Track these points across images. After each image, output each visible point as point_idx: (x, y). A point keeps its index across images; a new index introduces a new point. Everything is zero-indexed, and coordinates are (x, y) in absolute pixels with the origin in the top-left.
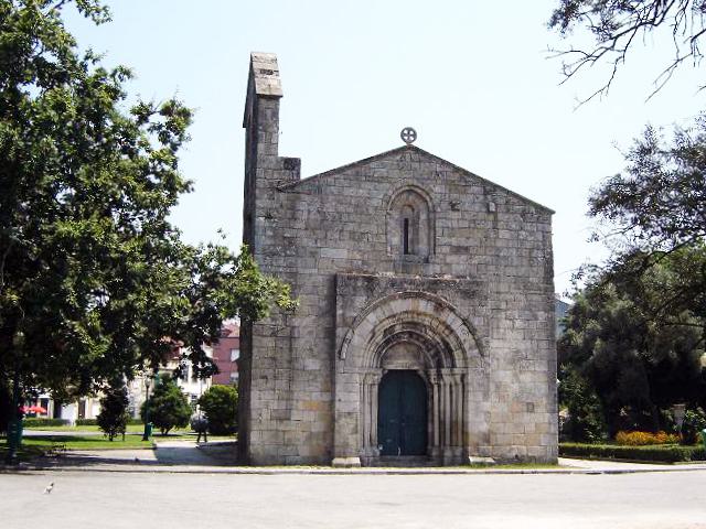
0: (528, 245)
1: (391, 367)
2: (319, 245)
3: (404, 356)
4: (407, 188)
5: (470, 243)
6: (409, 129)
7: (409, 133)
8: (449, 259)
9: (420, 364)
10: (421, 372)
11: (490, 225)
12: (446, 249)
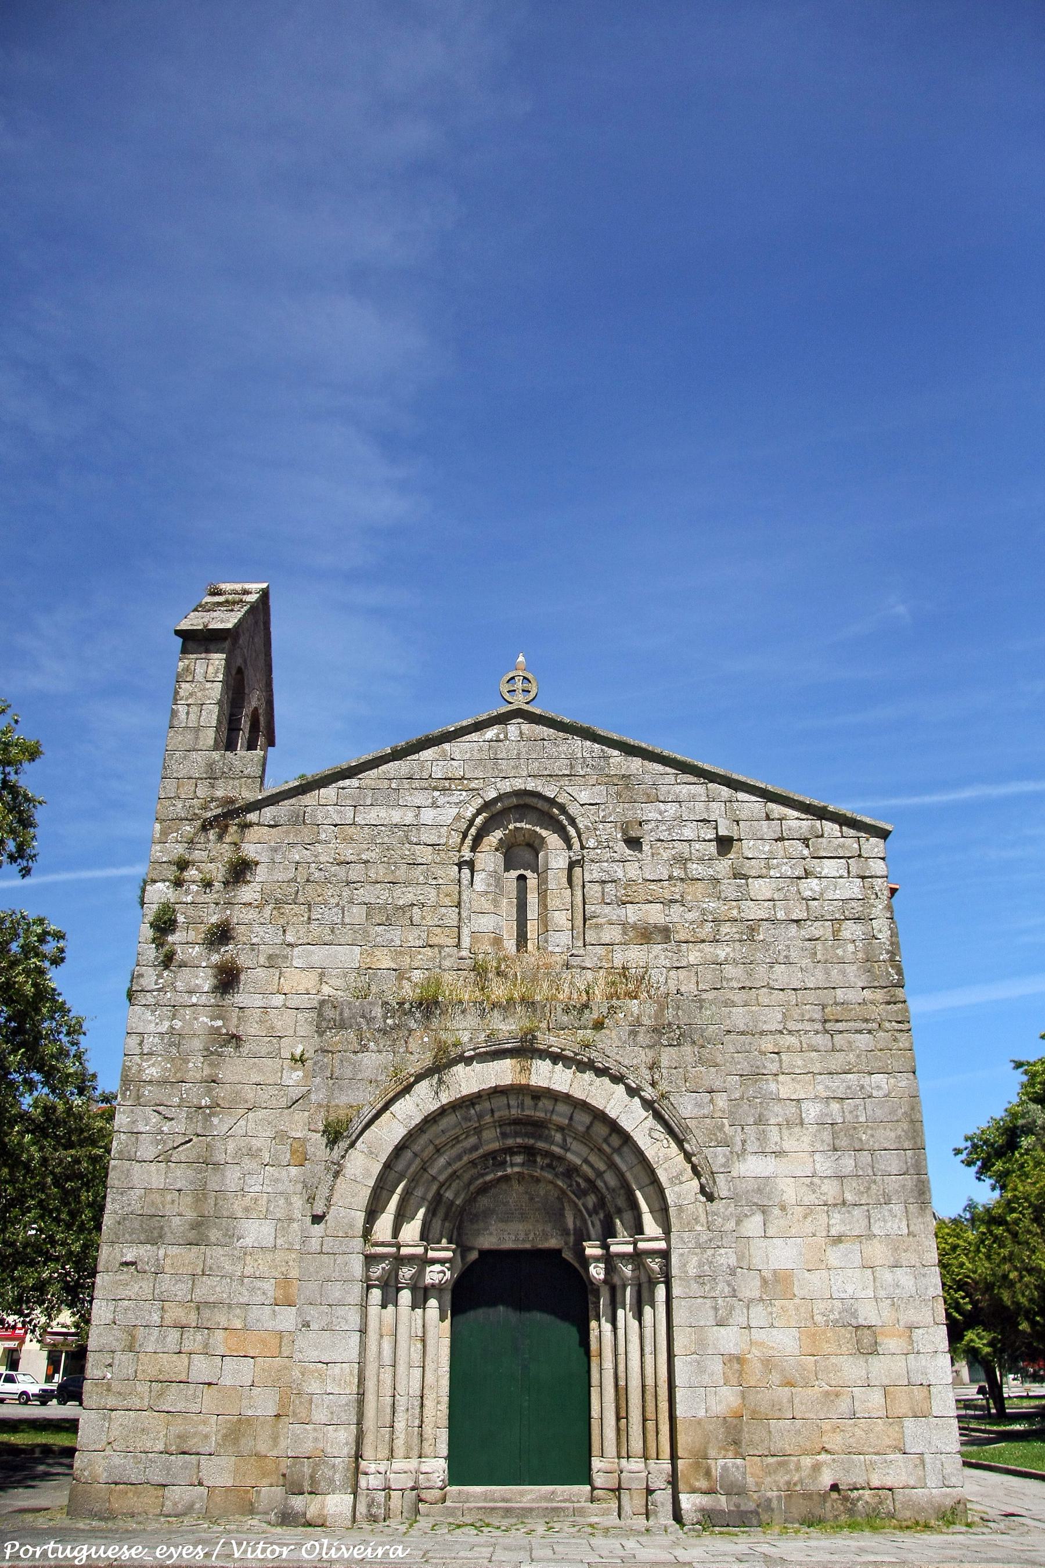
1: (488, 1241)
2: (290, 939)
3: (523, 1218)
9: (565, 1232)
10: (567, 1255)
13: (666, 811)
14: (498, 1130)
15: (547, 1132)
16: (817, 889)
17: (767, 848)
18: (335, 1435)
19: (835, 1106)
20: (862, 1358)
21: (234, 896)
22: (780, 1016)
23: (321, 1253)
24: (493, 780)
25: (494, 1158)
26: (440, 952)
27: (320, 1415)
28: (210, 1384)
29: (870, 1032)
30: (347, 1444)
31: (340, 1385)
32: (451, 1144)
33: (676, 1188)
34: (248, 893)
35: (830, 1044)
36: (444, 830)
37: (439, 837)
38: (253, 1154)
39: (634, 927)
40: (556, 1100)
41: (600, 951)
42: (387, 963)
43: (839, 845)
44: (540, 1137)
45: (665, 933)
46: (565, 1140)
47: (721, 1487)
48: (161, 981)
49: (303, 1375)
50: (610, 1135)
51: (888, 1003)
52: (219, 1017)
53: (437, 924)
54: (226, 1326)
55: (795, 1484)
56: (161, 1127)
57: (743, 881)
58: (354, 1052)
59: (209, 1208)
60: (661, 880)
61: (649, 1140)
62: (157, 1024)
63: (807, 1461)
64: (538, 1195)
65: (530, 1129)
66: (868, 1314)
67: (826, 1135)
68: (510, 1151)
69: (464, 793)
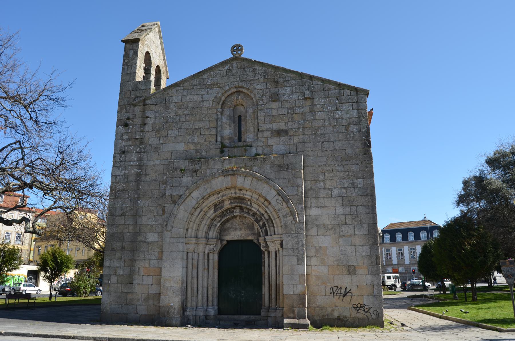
0: (344, 122)
1: (229, 238)
2: (161, 142)
3: (241, 229)
4: (235, 90)
5: (290, 126)
6: (239, 46)
7: (237, 48)
8: (271, 142)
9: (254, 234)
10: (255, 241)
11: (307, 109)
12: (268, 134)
13: (287, 90)
14: (229, 201)
15: (245, 201)
16: (341, 114)
17: (323, 101)
18: (175, 299)
19: (344, 191)
20: (350, 276)
21: (143, 129)
22: (325, 160)
23: (170, 243)
24: (228, 83)
25: (230, 211)
26: (210, 143)
27: (170, 294)
28: (139, 284)
29: (357, 164)
30: (178, 302)
31: (176, 284)
32: (211, 206)
33: (285, 219)
34: (147, 128)
35: (343, 169)
36: (211, 102)
37: (209, 104)
38: (151, 211)
39: (275, 131)
40: (247, 191)
41: (263, 140)
42: (192, 148)
43: (349, 98)
44: (243, 203)
45: (285, 132)
46: (251, 203)
47: (298, 317)
48: (121, 158)
49: (165, 281)
50: (265, 201)
51: (365, 154)
52: (140, 169)
53: (209, 134)
54: (143, 266)
55: (325, 316)
56: (123, 205)
57: (314, 113)
58: (180, 178)
59: (138, 230)
60: (285, 114)
61: (276, 203)
62: (120, 172)
63: (329, 310)
64: (245, 222)
65: (240, 200)
66: (353, 262)
67: (340, 201)
68: (234, 208)
69: (218, 88)
